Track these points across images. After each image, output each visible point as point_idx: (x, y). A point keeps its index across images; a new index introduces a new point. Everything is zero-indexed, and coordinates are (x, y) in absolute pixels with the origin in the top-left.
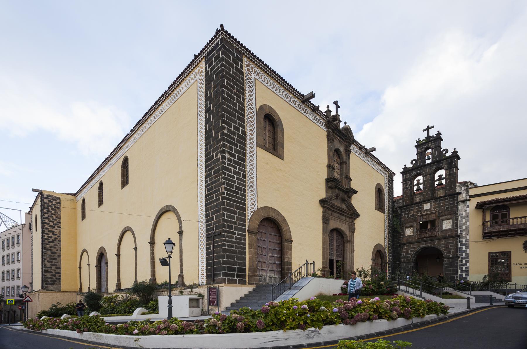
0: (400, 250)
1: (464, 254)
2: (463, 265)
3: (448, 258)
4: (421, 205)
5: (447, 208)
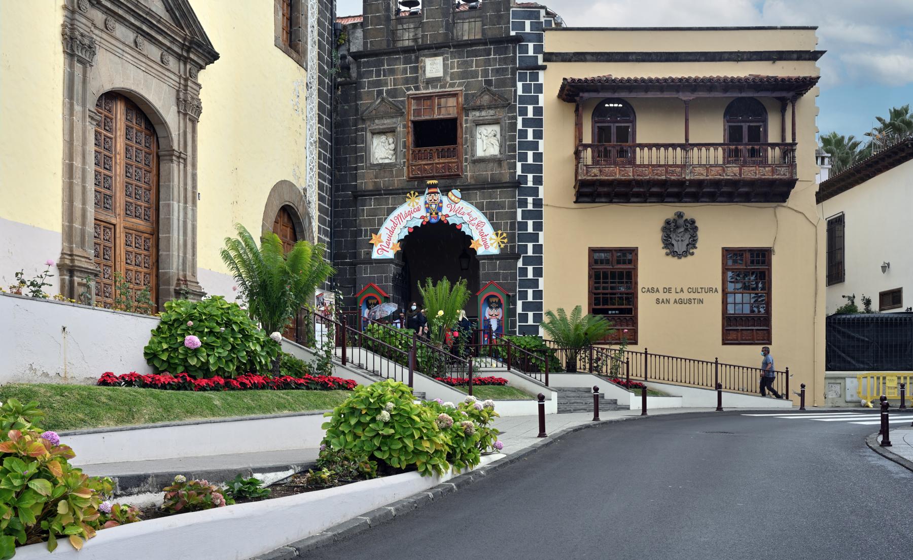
4: (417, 61)
5: (489, 83)
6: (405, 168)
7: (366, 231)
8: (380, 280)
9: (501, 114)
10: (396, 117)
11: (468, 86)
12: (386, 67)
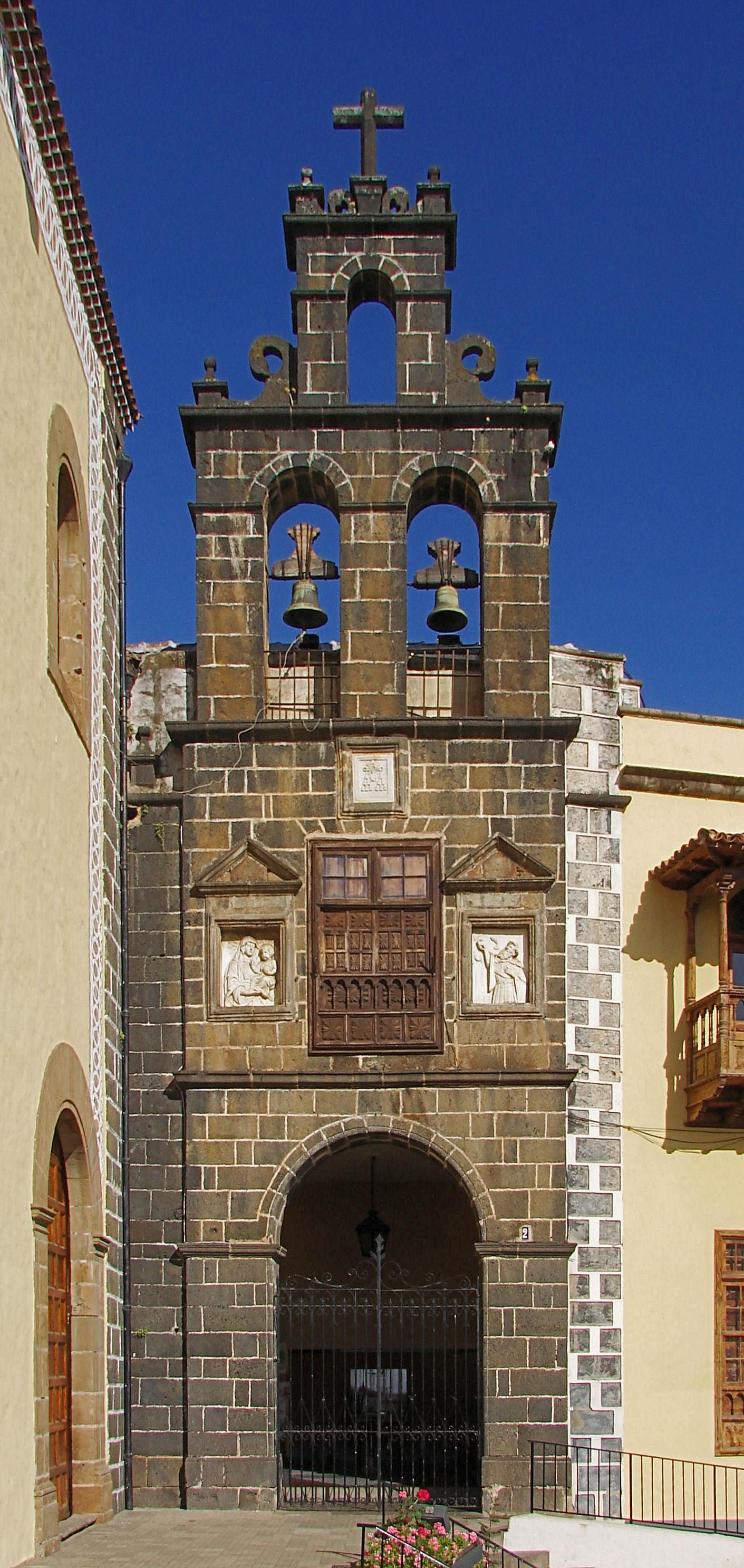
1: (594, 1223)
2: (586, 1314)
5: (500, 825)
7: (209, 1172)
8: (246, 1296)
12: (255, 768)
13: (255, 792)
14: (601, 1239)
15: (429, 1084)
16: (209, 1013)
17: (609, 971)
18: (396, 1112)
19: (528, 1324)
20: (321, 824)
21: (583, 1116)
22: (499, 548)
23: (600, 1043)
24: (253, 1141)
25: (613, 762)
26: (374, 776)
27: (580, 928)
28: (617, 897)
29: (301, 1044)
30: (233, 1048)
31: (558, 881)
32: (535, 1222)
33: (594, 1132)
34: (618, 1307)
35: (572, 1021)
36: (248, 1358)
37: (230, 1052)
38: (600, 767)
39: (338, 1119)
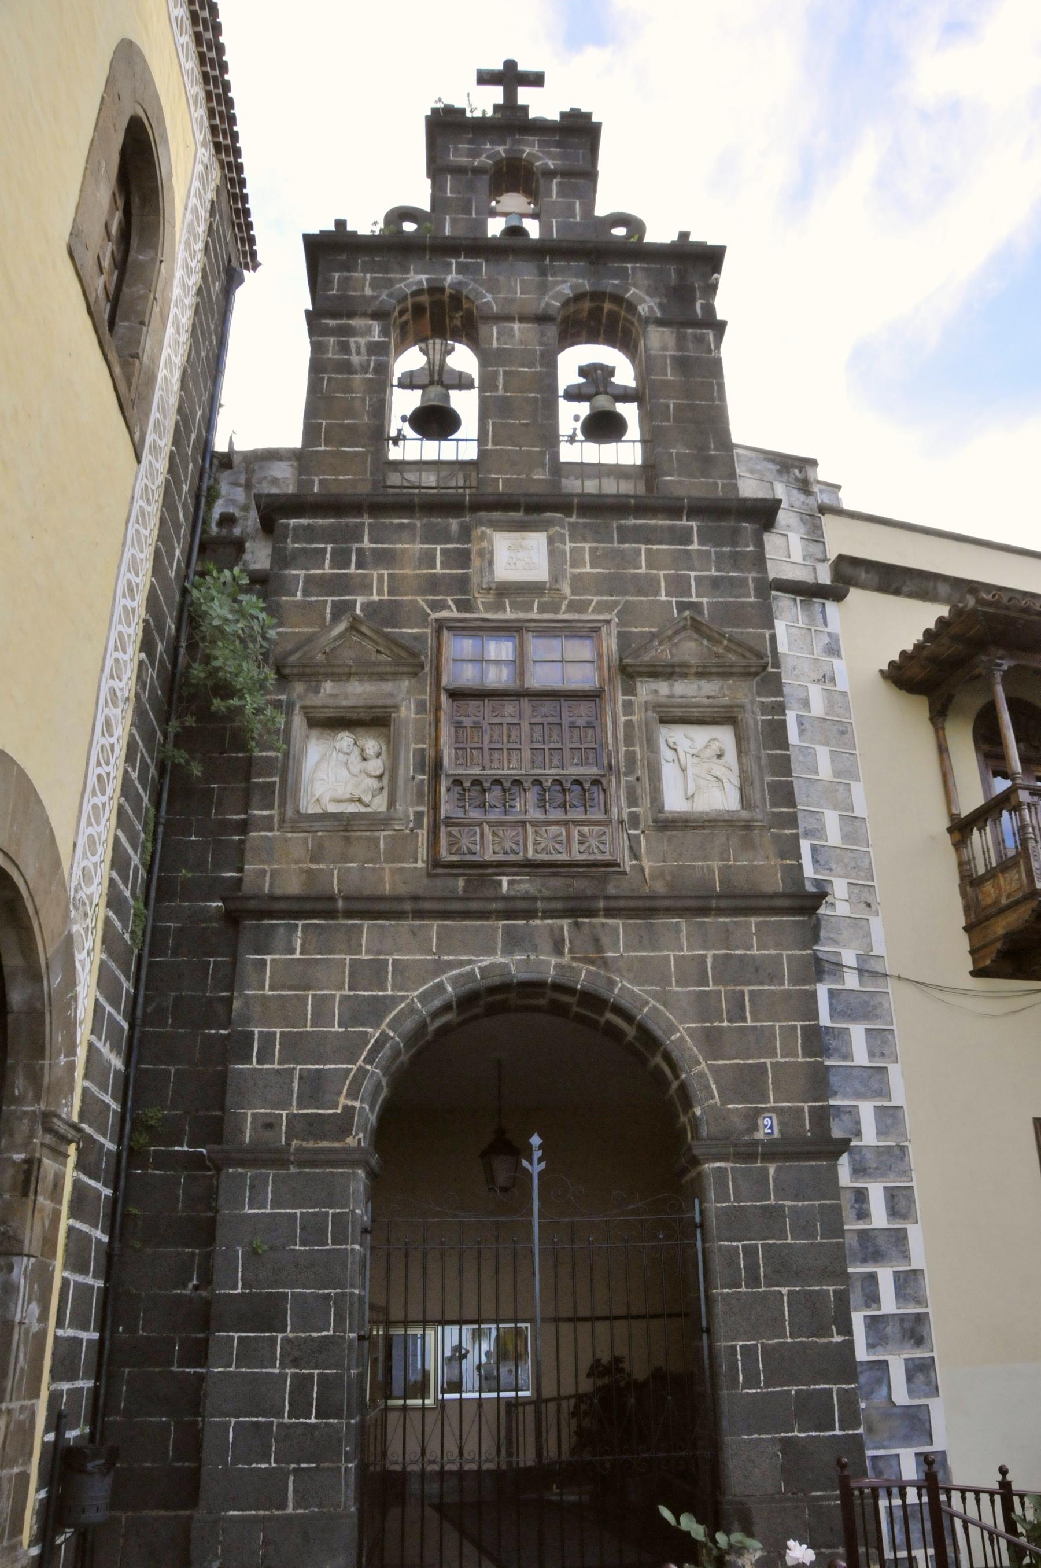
0: (231, 978)
1: (867, 1110)
2: (873, 1248)
3: (748, 1152)
4: (465, 534)
6: (423, 834)
7: (268, 1040)
8: (314, 1230)
9: (742, 693)
10: (395, 676)
11: (627, 613)
13: (364, 569)
14: (881, 1133)
15: (609, 913)
16: (282, 821)
17: (846, 778)
18: (559, 951)
19: (783, 1266)
20: (451, 603)
21: (833, 959)
22: (665, 357)
23: (846, 866)
24: (338, 994)
25: (820, 556)
26: (521, 554)
27: (803, 727)
28: (844, 694)
29: (416, 861)
30: (314, 866)
31: (770, 669)
32: (782, 1109)
33: (851, 981)
34: (915, 1235)
35: (807, 834)
36: (315, 1334)
37: (309, 872)
38: (804, 559)
39: (470, 962)
